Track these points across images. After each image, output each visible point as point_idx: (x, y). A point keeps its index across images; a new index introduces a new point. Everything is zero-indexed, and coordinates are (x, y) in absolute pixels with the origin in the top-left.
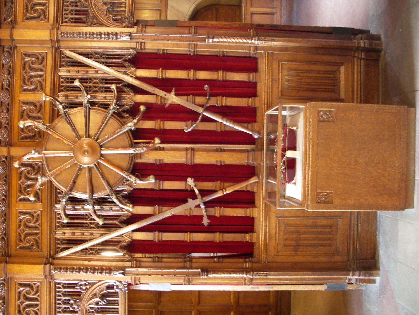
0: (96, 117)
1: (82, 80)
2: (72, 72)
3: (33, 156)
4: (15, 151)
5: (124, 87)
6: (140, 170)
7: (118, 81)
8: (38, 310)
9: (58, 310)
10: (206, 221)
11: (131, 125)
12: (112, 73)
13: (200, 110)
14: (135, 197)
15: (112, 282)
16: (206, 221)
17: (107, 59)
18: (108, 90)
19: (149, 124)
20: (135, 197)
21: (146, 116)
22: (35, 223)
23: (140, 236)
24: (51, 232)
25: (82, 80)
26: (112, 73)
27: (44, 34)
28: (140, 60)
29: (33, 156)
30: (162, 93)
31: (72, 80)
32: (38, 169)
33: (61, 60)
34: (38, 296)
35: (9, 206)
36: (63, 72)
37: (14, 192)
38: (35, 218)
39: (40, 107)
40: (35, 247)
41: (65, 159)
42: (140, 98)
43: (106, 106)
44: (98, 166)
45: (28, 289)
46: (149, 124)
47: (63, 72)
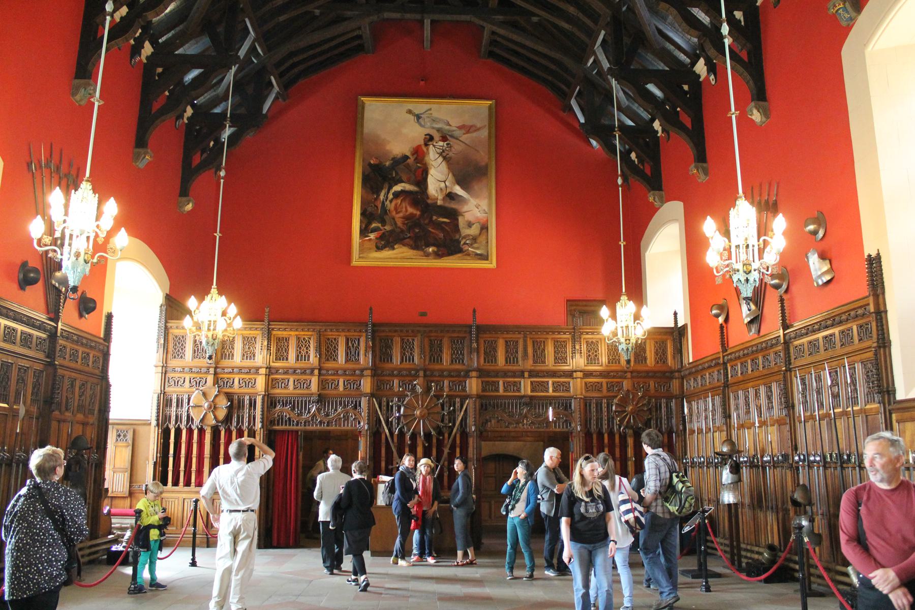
0: (439, 417)
1: (454, 410)
2: (458, 405)
3: (419, 389)
4: (421, 379)
5: (452, 428)
6: (414, 436)
7: (454, 425)
10: (390, 467)
11: (433, 433)
12: (458, 423)
13: (442, 463)
14: (402, 434)
15: (362, 424)
16: (390, 467)
17: (464, 419)
18: (450, 422)
19: (434, 441)
20: (402, 434)
21: (438, 439)
23: (383, 437)
24: (385, 396)
25: (454, 410)
26: (458, 423)
27: (474, 391)
28: (464, 435)
29: (419, 389)
30: (449, 446)
31: (454, 406)
32: (413, 389)
33: (463, 399)
35: (396, 376)
36: (458, 400)
37: (403, 378)
39: (442, 389)
41: (418, 403)
42: (446, 435)
43: (442, 421)
44: (415, 419)
46: (434, 441)
47: (458, 400)
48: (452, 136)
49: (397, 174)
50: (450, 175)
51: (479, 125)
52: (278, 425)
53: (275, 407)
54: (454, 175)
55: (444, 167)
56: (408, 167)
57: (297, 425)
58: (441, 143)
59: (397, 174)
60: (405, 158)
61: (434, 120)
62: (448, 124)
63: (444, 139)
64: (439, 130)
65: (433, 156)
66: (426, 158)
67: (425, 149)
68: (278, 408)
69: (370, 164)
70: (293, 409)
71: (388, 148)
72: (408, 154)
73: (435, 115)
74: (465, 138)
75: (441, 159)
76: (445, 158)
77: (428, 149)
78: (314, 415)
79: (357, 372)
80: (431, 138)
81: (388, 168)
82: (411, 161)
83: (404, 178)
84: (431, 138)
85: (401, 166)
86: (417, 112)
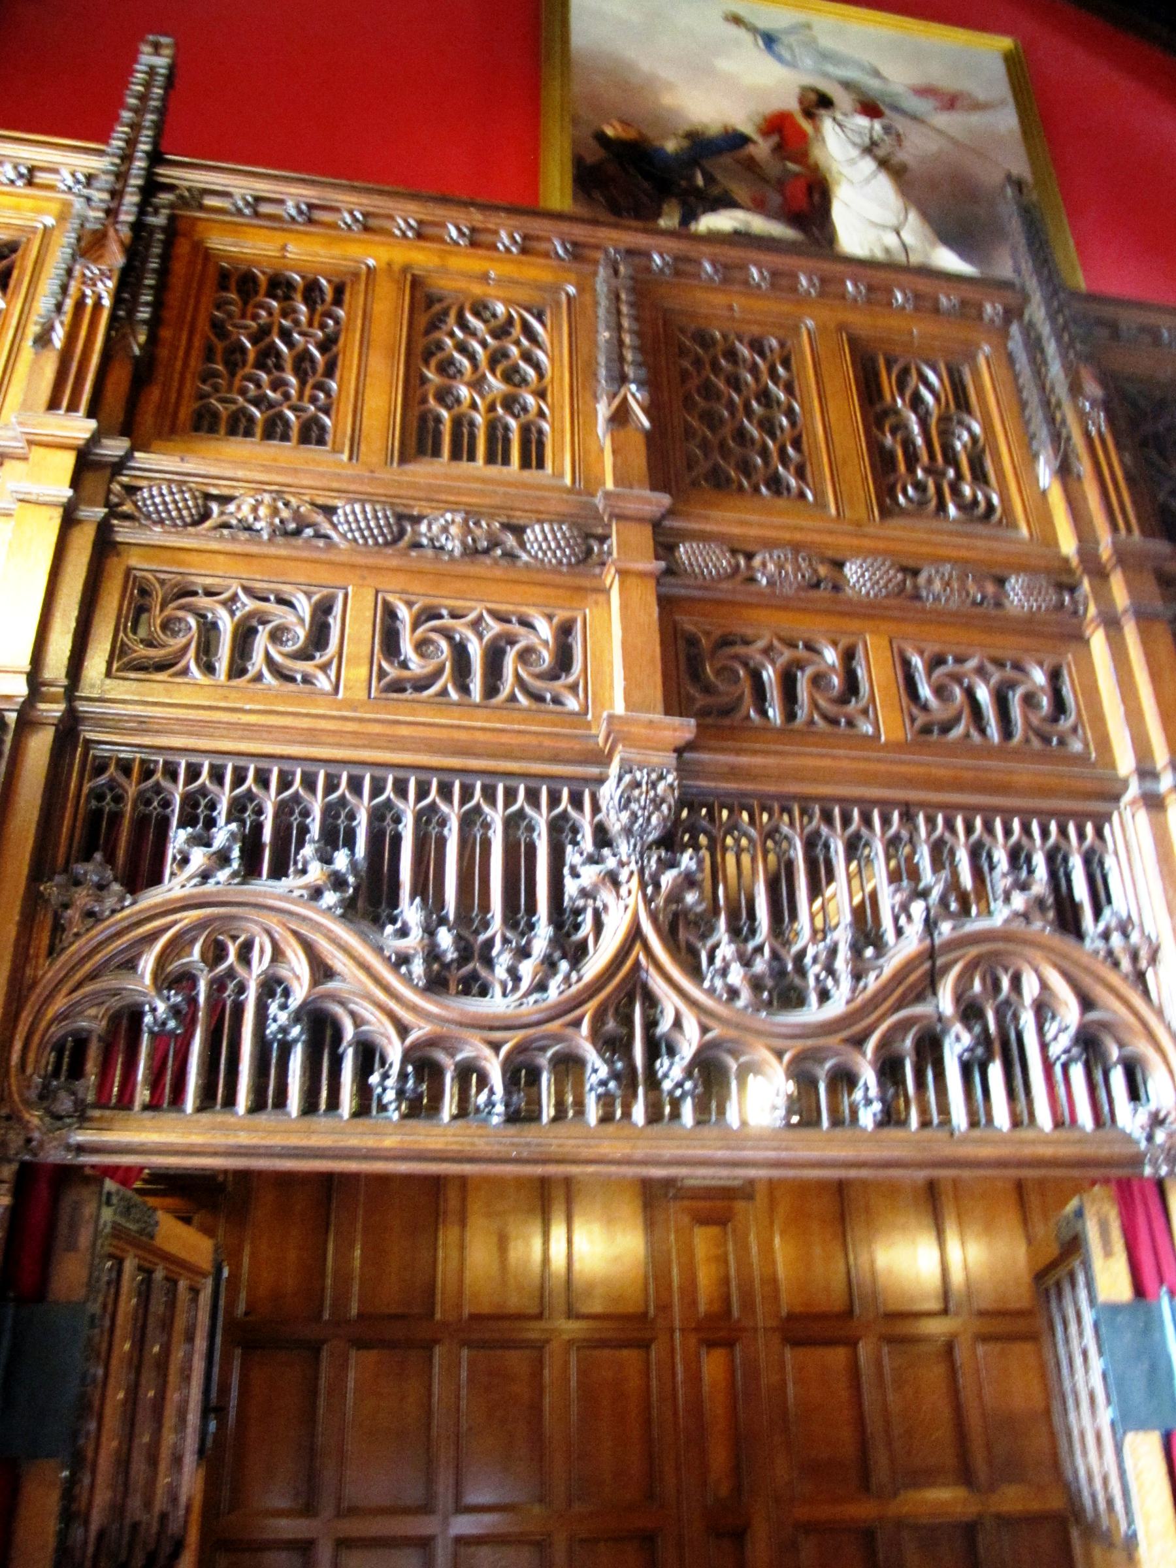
8: (444, 692)
9: (978, 822)
22: (269, 660)
34: (512, 698)
38: (289, 663)
40: (393, 672)
45: (546, 654)
48: (896, 109)
49: (710, 179)
50: (913, 216)
51: (981, 96)
52: (166, 1096)
53: (144, 871)
54: (925, 215)
55: (884, 185)
56: (751, 165)
57: (421, 1107)
58: (862, 121)
59: (710, 179)
60: (735, 140)
61: (825, 56)
62: (877, 74)
63: (870, 109)
64: (847, 85)
65: (838, 146)
66: (817, 153)
67: (806, 125)
68: (175, 886)
69: (601, 138)
70: (371, 900)
71: (667, 100)
72: (748, 129)
73: (826, 42)
74: (942, 120)
75: (868, 165)
76: (884, 164)
77: (817, 130)
78: (626, 993)
79: (1018, 594)
80: (825, 102)
81: (677, 156)
82: (762, 148)
83: (740, 192)
84: (825, 102)
85: (726, 159)
86: (763, 24)
